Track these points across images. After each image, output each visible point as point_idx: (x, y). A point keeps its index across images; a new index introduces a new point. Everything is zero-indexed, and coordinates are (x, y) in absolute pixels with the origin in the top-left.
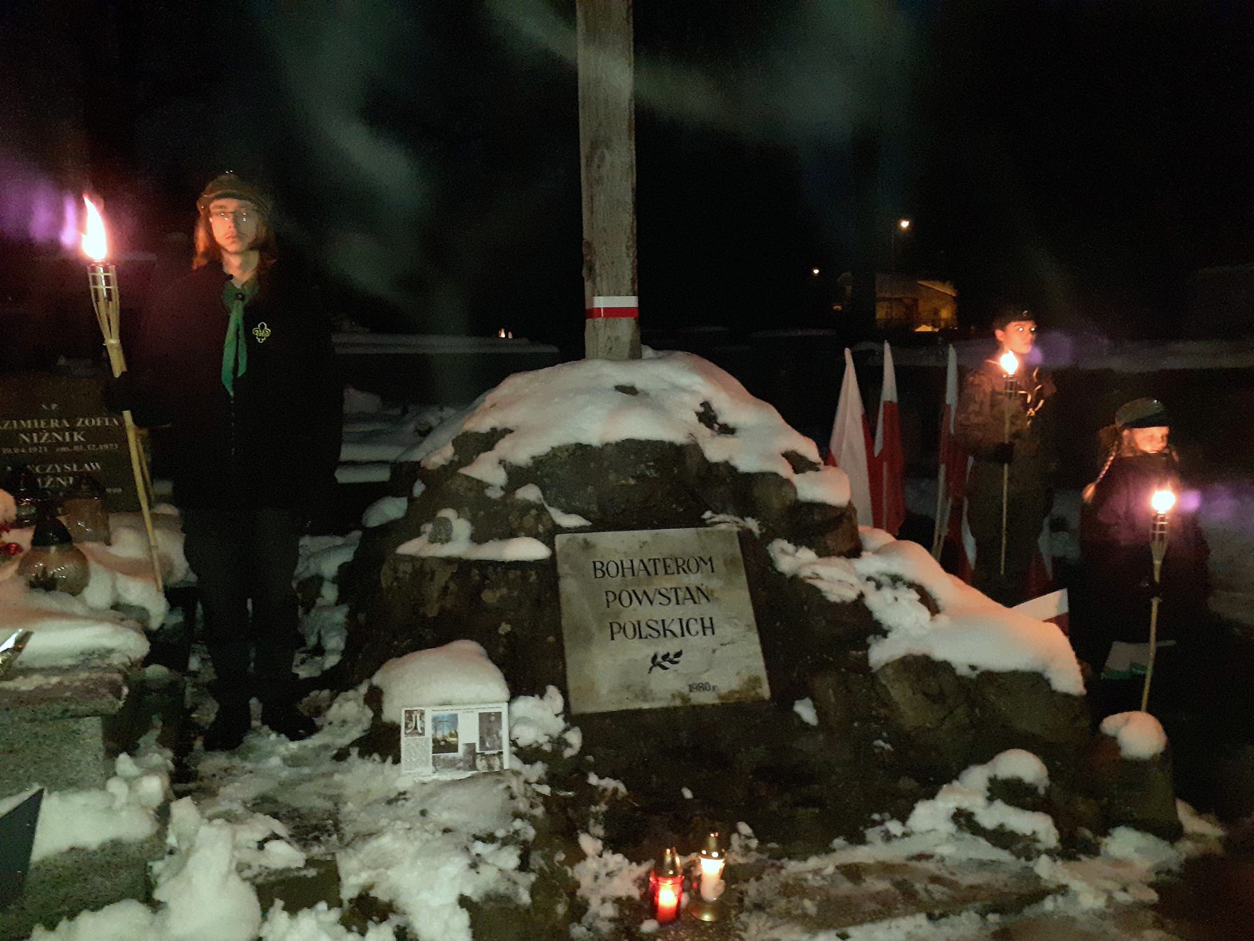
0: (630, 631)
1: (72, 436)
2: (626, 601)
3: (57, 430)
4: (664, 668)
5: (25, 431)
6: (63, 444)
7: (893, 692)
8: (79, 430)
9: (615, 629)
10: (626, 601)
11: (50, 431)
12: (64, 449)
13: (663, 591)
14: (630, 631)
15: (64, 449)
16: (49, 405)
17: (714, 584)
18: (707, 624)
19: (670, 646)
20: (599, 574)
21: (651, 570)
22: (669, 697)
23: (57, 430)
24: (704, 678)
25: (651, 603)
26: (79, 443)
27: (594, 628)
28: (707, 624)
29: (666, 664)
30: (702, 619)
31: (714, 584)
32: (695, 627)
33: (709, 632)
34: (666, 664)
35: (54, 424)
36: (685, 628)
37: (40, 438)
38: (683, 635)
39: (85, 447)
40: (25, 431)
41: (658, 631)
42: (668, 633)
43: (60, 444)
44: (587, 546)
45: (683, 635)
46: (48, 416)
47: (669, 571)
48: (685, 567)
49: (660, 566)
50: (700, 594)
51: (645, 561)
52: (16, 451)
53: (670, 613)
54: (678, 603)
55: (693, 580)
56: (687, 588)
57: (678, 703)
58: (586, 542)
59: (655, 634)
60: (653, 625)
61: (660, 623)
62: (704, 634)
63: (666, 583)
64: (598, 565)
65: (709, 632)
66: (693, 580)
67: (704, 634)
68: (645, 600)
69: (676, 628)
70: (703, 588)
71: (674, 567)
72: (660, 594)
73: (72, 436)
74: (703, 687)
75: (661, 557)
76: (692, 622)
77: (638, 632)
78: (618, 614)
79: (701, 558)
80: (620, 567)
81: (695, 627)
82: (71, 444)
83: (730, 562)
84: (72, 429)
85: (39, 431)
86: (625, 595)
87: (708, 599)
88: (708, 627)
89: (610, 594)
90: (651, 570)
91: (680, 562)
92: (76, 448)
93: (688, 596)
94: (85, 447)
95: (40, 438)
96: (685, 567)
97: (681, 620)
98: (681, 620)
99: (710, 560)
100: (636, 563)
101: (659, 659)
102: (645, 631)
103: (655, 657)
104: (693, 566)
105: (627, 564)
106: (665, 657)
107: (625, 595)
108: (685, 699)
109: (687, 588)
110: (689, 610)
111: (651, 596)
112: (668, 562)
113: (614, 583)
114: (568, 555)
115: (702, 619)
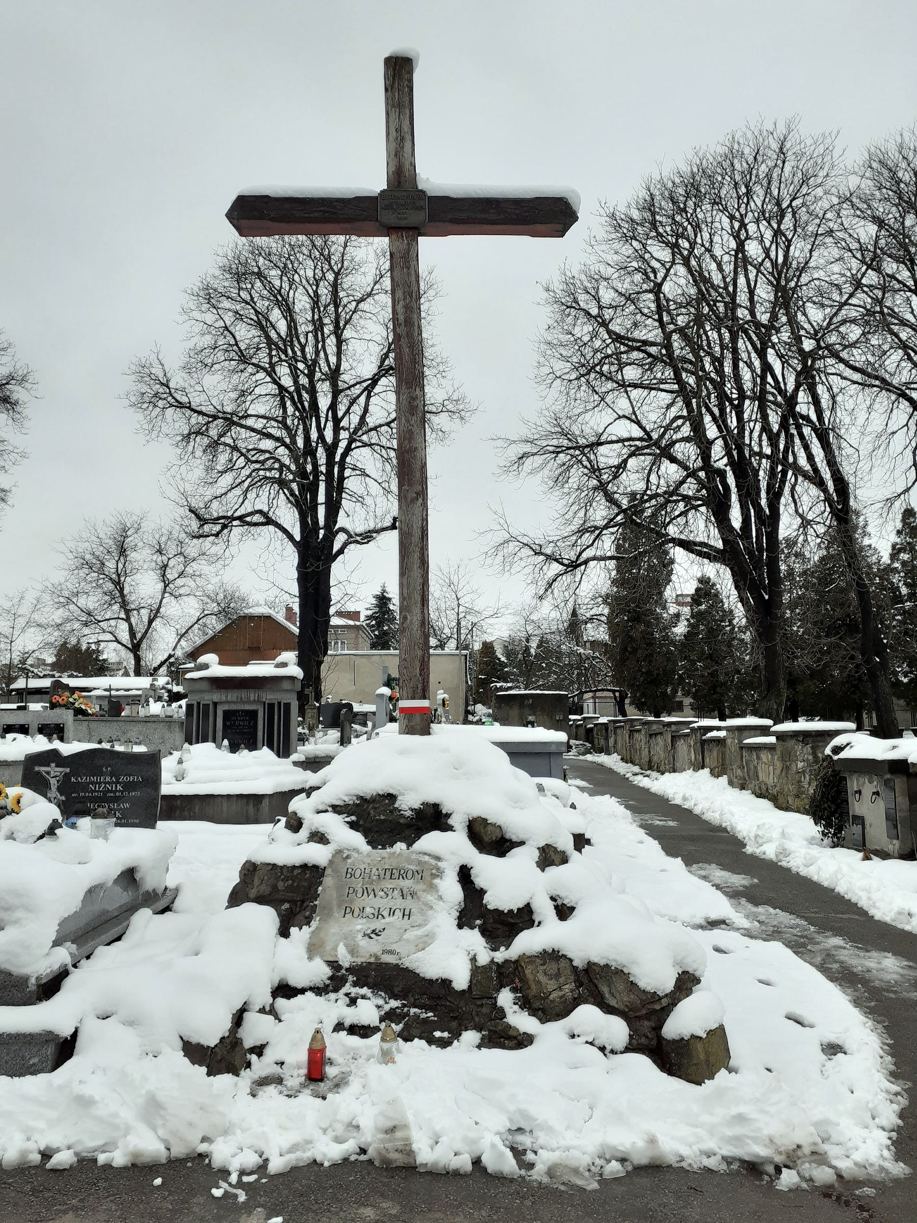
2: (359, 895)
4: (370, 938)
5: (92, 783)
6: (111, 791)
7: (527, 972)
9: (348, 911)
10: (359, 895)
11: (105, 783)
18: (407, 912)
19: (378, 924)
20: (349, 875)
21: (382, 876)
22: (368, 955)
23: (109, 783)
24: (393, 947)
27: (335, 908)
28: (407, 912)
29: (372, 936)
33: (406, 917)
34: (372, 936)
40: (92, 783)
43: (109, 791)
49: (389, 874)
52: (87, 794)
55: (406, 884)
57: (372, 960)
63: (388, 884)
64: (350, 870)
65: (406, 917)
68: (372, 895)
69: (385, 913)
71: (396, 875)
74: (391, 952)
76: (398, 911)
78: (352, 901)
81: (399, 914)
82: (115, 792)
84: (117, 782)
85: (100, 783)
89: (351, 891)
90: (382, 876)
91: (402, 872)
92: (117, 794)
100: (374, 870)
104: (410, 874)
106: (373, 931)
108: (377, 957)
111: (376, 892)
112: (394, 871)
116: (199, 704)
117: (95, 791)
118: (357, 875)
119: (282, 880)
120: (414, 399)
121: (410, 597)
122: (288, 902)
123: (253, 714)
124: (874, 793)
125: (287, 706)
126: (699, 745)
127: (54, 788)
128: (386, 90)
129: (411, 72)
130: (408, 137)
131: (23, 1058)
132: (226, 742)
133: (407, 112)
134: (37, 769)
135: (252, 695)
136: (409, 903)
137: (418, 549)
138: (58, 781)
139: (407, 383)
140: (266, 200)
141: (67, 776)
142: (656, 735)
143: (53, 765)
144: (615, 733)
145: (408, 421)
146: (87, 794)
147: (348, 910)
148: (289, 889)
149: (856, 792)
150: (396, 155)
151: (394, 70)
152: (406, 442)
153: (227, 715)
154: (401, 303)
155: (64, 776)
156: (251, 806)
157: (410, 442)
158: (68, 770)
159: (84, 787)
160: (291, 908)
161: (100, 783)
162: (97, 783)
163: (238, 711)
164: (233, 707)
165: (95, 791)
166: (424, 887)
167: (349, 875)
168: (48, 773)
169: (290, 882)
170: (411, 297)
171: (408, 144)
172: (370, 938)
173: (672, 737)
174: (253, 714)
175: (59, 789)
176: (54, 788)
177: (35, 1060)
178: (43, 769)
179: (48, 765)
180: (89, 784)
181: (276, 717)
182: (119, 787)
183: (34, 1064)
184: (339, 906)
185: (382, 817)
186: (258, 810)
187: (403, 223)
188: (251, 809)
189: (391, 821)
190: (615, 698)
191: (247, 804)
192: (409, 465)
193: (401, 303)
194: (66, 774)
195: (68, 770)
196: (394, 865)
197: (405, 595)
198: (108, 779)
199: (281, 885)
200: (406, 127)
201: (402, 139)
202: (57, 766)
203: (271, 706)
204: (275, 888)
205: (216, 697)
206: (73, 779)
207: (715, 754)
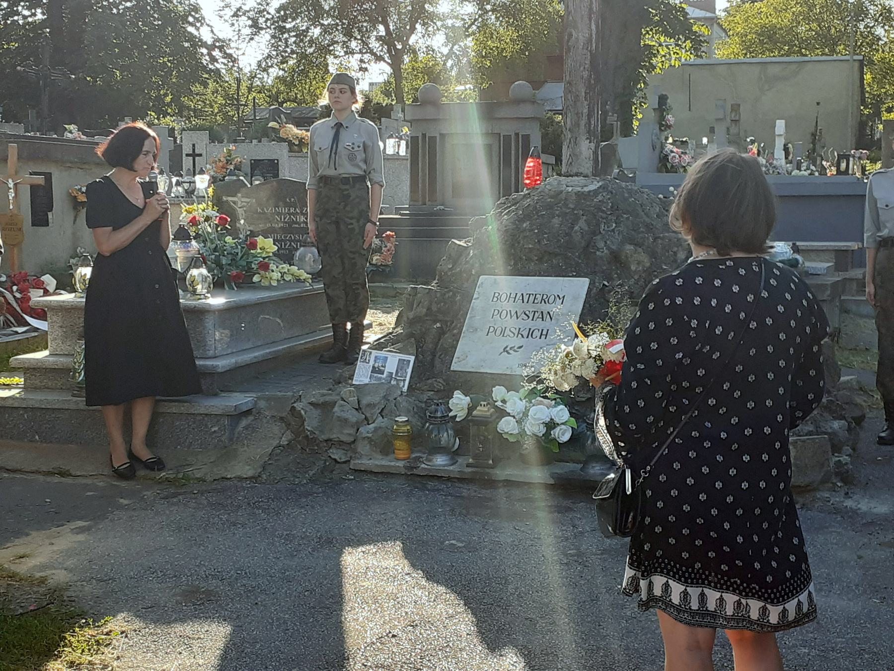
0: (498, 332)
4: (509, 353)
13: (527, 313)
14: (498, 332)
18: (544, 333)
21: (525, 300)
25: (517, 318)
28: (544, 333)
30: (542, 330)
32: (537, 334)
34: (511, 352)
38: (528, 337)
41: (514, 334)
42: (520, 335)
45: (528, 337)
47: (536, 301)
48: (546, 300)
49: (532, 298)
50: (548, 316)
51: (524, 295)
54: (533, 320)
55: (545, 308)
56: (542, 312)
57: (508, 372)
59: (512, 335)
61: (517, 330)
62: (540, 338)
65: (543, 337)
66: (545, 308)
67: (540, 338)
69: (525, 333)
70: (551, 313)
72: (525, 314)
75: (534, 293)
79: (558, 296)
81: (537, 334)
83: (575, 298)
87: (551, 319)
90: (525, 300)
93: (541, 316)
96: (546, 300)
97: (530, 329)
98: (530, 329)
99: (564, 297)
101: (508, 349)
102: (507, 332)
103: (507, 347)
105: (513, 296)
106: (511, 349)
109: (542, 312)
111: (518, 314)
115: (542, 330)
136: (546, 324)
172: (509, 353)
185: (530, 246)
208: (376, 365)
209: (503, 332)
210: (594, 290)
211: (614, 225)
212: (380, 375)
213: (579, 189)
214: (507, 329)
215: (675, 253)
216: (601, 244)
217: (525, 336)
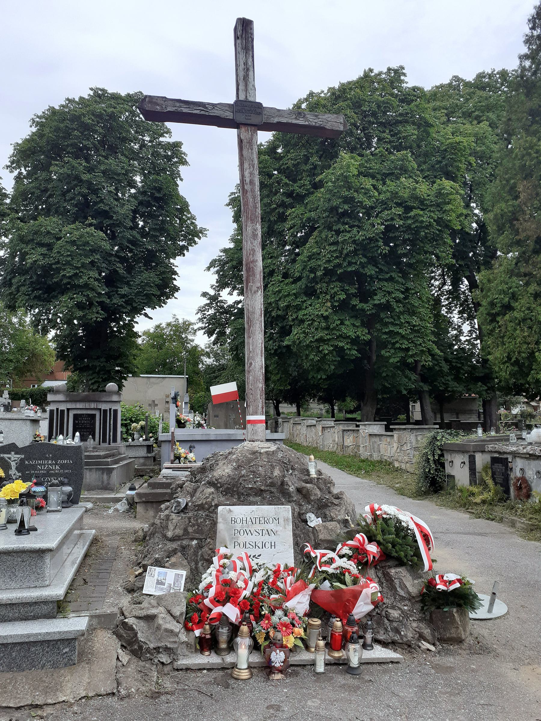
0: (242, 545)
1: (55, 467)
2: (242, 534)
3: (51, 465)
5: (40, 465)
6: (52, 470)
8: (58, 465)
10: (242, 534)
12: (53, 472)
13: (257, 530)
15: (53, 472)
16: (49, 455)
17: (280, 528)
18: (273, 544)
20: (233, 522)
21: (254, 522)
23: (51, 465)
26: (58, 470)
28: (273, 544)
31: (280, 528)
32: (268, 545)
33: (273, 547)
35: (50, 462)
36: (263, 546)
37: (44, 467)
39: (59, 471)
40: (40, 465)
43: (50, 470)
44: (230, 511)
46: (47, 459)
48: (268, 521)
49: (258, 520)
52: (36, 472)
53: (259, 539)
58: (230, 510)
60: (252, 544)
63: (258, 527)
64: (233, 519)
65: (273, 547)
71: (263, 521)
73: (55, 467)
77: (245, 545)
78: (238, 538)
80: (242, 520)
81: (268, 545)
84: (56, 464)
85: (45, 464)
86: (242, 531)
88: (273, 545)
89: (236, 532)
90: (254, 522)
92: (56, 472)
94: (59, 471)
95: (44, 467)
96: (268, 521)
102: (248, 545)
106: (254, 556)
107: (242, 531)
110: (266, 538)
113: (238, 526)
114: (222, 514)
116: (57, 409)
117: (42, 470)
118: (238, 521)
119: (191, 526)
120: (255, 231)
121: (254, 352)
122: (197, 539)
123: (94, 416)
124: (462, 463)
125: (116, 411)
126: (341, 432)
127: (14, 468)
128: (236, 38)
129: (252, 29)
130: (251, 69)
131: (59, 649)
132: (78, 434)
133: (251, 53)
134: (2, 455)
135: (93, 405)
136: (273, 538)
137: (258, 322)
138: (16, 464)
139: (251, 220)
140: (164, 99)
141: (22, 460)
142: (311, 426)
143: (13, 453)
144: (283, 425)
145: (252, 243)
146: (36, 472)
147: (236, 544)
148: (195, 532)
149: (450, 462)
150: (244, 79)
151: (243, 26)
152: (251, 256)
153: (76, 417)
154: (248, 171)
155: (20, 460)
156: (105, 474)
157: (253, 256)
158: (23, 456)
159: (34, 467)
160: (198, 543)
161: (45, 464)
162: (42, 464)
163: (83, 414)
164: (79, 412)
165: (42, 470)
166: (281, 528)
167: (233, 522)
168: (10, 458)
169: (196, 527)
170: (253, 167)
171: (251, 73)
173: (323, 427)
174: (94, 416)
175: (17, 468)
176: (14, 468)
177: (67, 650)
178: (6, 456)
179: (10, 454)
180: (37, 465)
181: (108, 418)
182: (57, 467)
183: (66, 652)
184: (231, 541)
185: (250, 486)
186: (110, 477)
187: (249, 122)
188: (105, 477)
189: (255, 488)
190: (274, 404)
191: (103, 473)
192: (253, 271)
193: (248, 171)
194: (22, 458)
195: (23, 456)
196: (261, 515)
197: (251, 350)
198: (50, 462)
199: (190, 530)
200: (250, 63)
201: (248, 70)
202: (15, 454)
203: (105, 411)
204: (185, 530)
205: (69, 406)
206: (26, 462)
207: (351, 438)
208: (159, 579)
209: (245, 545)
210: (296, 514)
211: (291, 471)
212: (162, 586)
213: (267, 450)
214: (247, 543)
215: (329, 487)
216: (290, 484)
217: (261, 547)
